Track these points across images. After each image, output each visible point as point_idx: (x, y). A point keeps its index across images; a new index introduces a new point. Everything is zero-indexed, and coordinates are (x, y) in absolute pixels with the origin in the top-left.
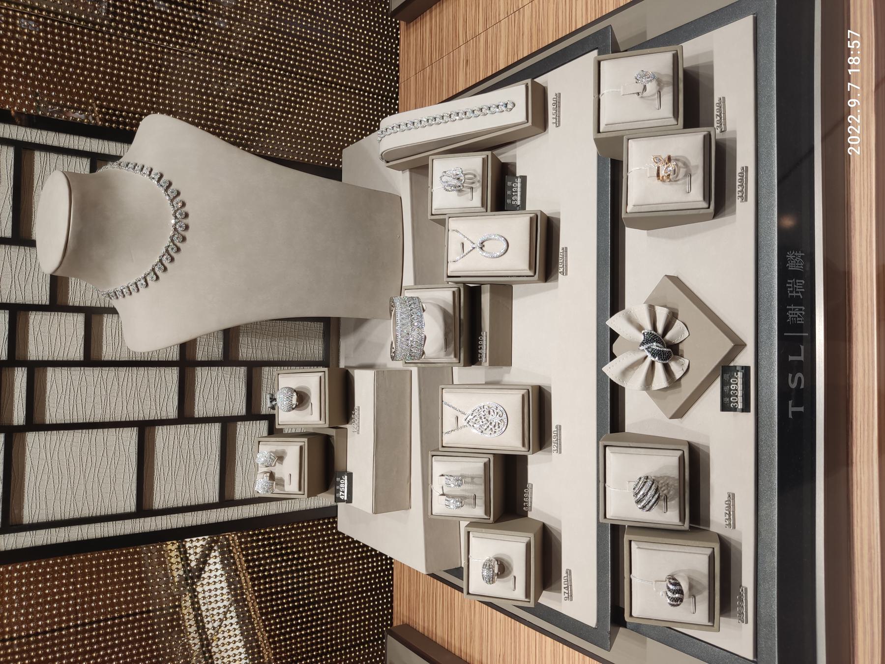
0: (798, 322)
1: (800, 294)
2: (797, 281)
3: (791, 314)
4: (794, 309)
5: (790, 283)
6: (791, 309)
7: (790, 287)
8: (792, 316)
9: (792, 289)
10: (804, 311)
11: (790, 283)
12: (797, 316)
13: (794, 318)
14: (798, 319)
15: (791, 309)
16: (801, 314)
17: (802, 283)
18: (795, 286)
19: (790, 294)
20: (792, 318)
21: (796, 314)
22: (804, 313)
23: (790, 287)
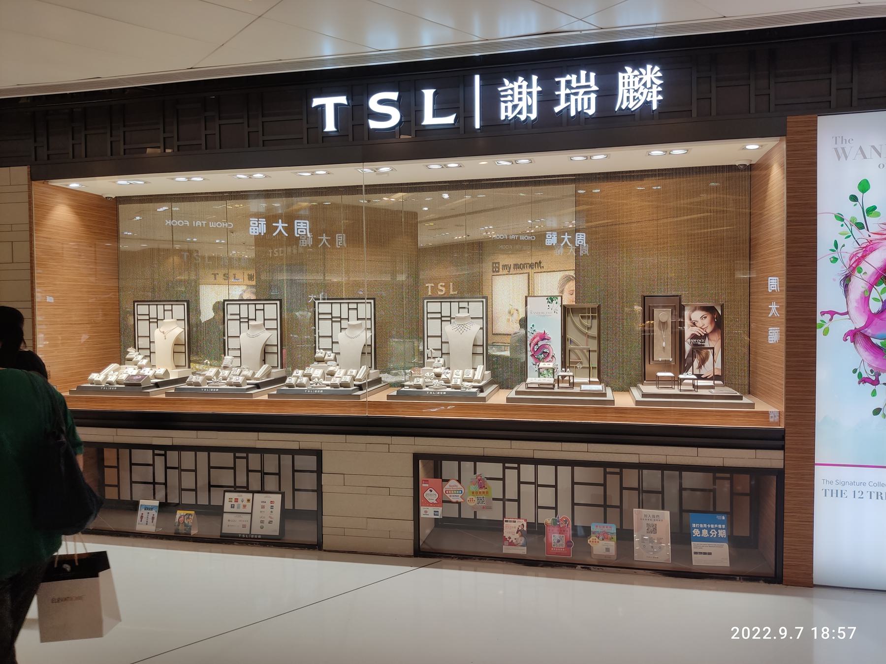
0: (503, 105)
1: (563, 105)
2: (593, 96)
3: (520, 87)
4: (530, 93)
5: (588, 79)
6: (529, 86)
7: (578, 80)
8: (517, 90)
9: (574, 84)
10: (528, 117)
11: (588, 79)
12: (516, 102)
13: (512, 95)
14: (510, 105)
15: (529, 86)
16: (520, 113)
17: (589, 108)
18: (582, 91)
19: (563, 80)
20: (512, 89)
21: (520, 99)
22: (523, 117)
23: (578, 80)
